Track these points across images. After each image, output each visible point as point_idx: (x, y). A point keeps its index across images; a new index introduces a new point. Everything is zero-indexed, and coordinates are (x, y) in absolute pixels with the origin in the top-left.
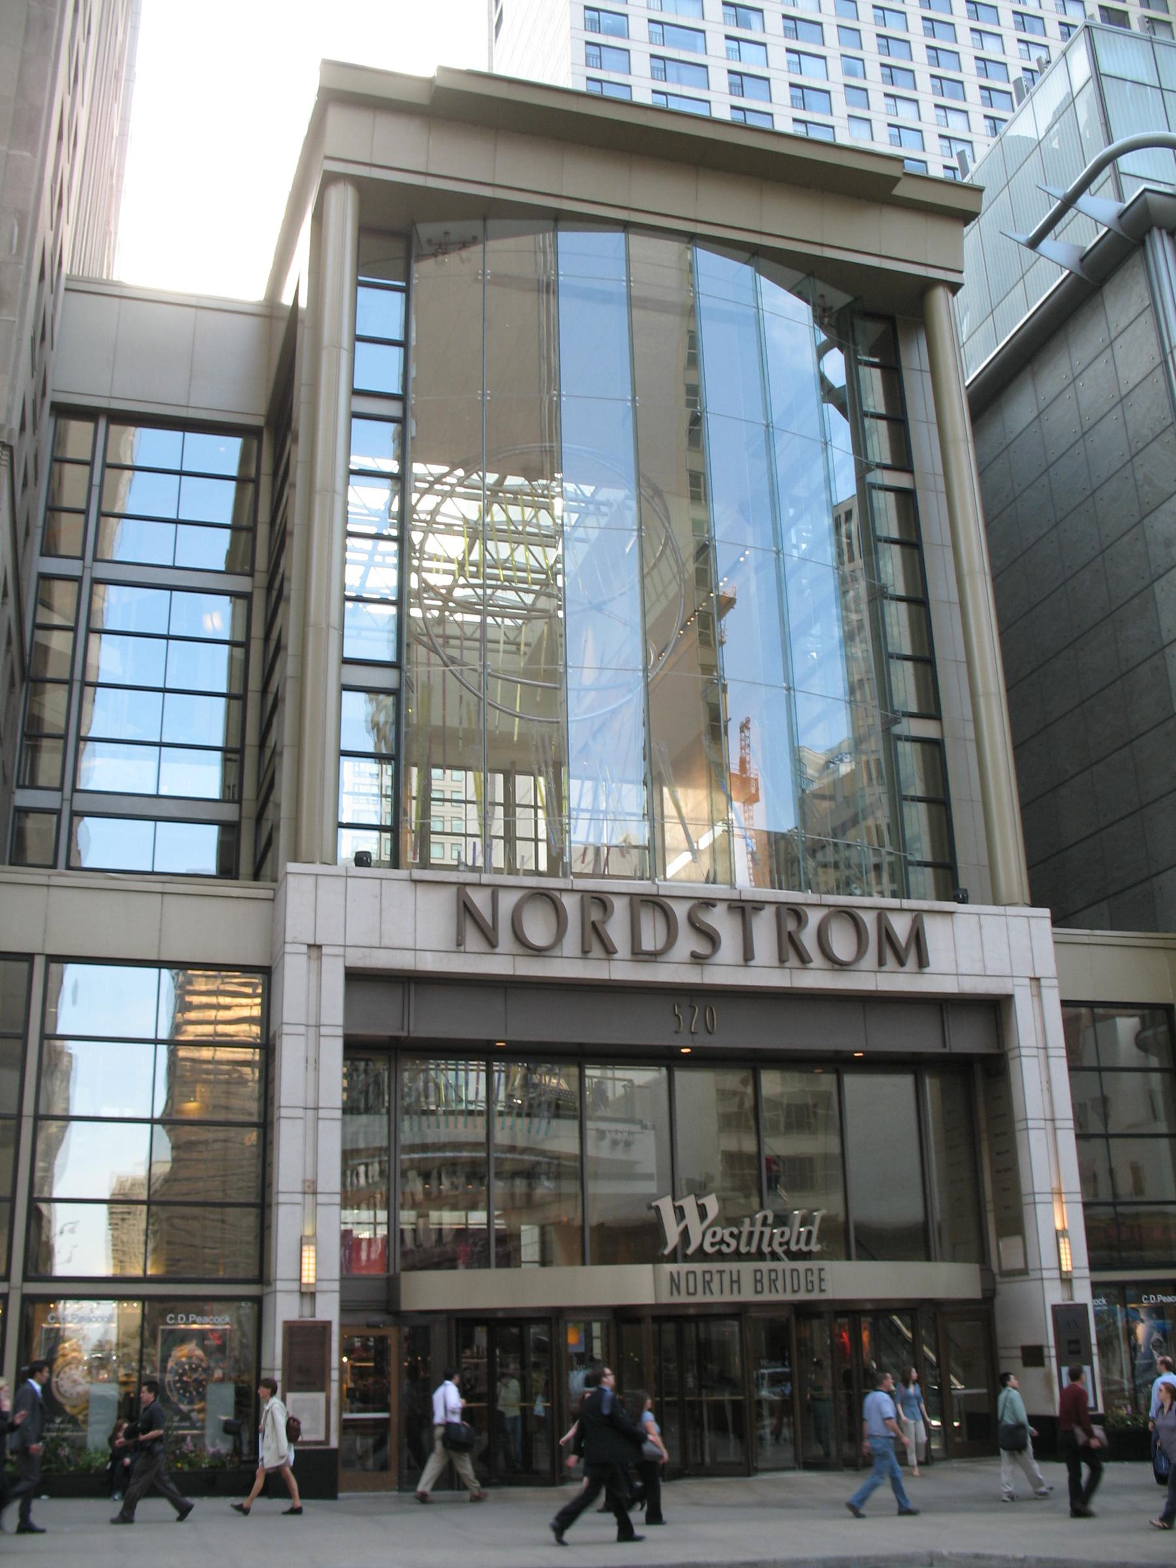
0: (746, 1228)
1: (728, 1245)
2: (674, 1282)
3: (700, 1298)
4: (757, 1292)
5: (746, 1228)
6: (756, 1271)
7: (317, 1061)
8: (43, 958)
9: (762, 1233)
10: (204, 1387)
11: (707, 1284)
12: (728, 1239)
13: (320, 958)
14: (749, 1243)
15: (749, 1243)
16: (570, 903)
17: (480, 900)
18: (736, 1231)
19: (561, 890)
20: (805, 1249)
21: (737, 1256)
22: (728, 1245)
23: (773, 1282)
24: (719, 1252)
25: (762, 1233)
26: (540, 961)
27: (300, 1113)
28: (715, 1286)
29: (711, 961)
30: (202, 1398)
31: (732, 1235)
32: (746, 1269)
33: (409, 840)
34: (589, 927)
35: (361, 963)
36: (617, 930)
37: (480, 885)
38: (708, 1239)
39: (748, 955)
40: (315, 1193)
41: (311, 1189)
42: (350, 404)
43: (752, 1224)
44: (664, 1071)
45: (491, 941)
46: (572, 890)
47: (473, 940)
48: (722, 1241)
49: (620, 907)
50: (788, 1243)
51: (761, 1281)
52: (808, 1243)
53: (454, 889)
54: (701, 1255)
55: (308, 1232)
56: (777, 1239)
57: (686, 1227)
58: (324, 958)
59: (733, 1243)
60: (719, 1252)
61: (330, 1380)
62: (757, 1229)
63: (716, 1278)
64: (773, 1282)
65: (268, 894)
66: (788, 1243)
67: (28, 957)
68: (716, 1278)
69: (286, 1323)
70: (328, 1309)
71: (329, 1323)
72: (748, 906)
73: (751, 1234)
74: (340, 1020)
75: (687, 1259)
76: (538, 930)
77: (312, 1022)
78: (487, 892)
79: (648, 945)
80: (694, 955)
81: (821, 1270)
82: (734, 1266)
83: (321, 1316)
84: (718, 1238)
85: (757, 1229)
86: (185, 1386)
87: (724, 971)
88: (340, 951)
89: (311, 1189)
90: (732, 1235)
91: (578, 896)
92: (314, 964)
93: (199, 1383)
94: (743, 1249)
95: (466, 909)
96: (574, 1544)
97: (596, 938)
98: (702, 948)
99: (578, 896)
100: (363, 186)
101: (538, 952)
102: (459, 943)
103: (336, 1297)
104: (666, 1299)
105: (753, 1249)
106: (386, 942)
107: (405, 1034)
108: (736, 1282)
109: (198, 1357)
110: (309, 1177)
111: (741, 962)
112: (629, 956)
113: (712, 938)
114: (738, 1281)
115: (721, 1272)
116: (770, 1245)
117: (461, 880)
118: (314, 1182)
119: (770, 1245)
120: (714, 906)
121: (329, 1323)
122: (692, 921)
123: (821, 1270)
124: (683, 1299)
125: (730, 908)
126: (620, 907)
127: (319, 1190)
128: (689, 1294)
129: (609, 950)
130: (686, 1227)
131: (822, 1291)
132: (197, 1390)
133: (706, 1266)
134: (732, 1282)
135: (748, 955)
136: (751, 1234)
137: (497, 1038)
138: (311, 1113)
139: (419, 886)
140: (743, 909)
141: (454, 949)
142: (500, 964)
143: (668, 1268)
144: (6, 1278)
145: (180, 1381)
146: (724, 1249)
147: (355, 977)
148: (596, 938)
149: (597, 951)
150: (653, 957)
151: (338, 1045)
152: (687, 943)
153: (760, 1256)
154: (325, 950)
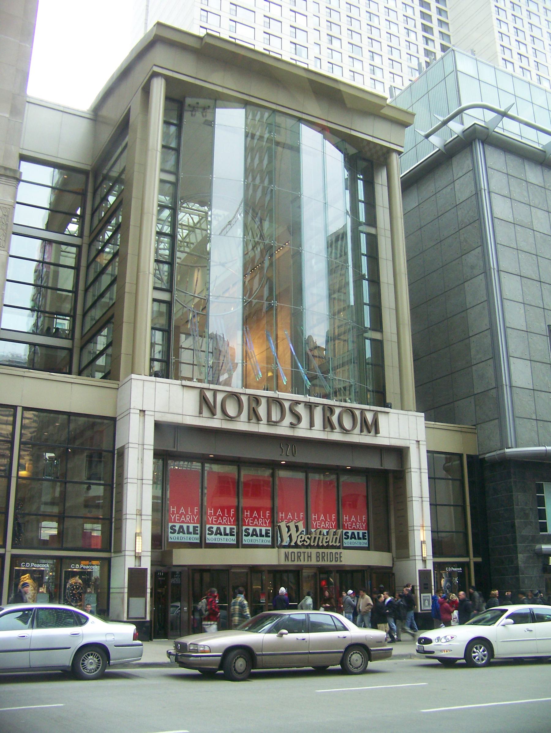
0: (313, 536)
1: (307, 542)
2: (286, 556)
3: (296, 563)
4: (317, 561)
5: (313, 536)
6: (317, 553)
7: (142, 459)
8: (21, 408)
9: (319, 538)
10: (81, 595)
11: (299, 557)
12: (306, 539)
13: (144, 415)
14: (314, 542)
15: (314, 542)
16: (244, 399)
17: (209, 395)
18: (310, 537)
19: (240, 393)
20: (335, 545)
21: (309, 546)
22: (307, 542)
23: (323, 557)
24: (303, 545)
25: (319, 538)
26: (274, 427)
27: (136, 481)
28: (302, 558)
29: (297, 426)
30: (81, 600)
31: (308, 538)
32: (314, 551)
33: (172, 368)
34: (327, 419)
35: (160, 419)
36: (262, 410)
37: (209, 389)
38: (299, 539)
39: (312, 424)
40: (141, 515)
41: (140, 513)
42: (159, 176)
43: (316, 534)
44: (365, 478)
45: (213, 413)
46: (245, 394)
47: (206, 412)
48: (304, 541)
49: (263, 401)
50: (328, 542)
51: (319, 557)
52: (335, 542)
53: (199, 390)
54: (296, 546)
55: (138, 531)
56: (325, 540)
57: (291, 534)
58: (146, 416)
59: (308, 541)
60: (303, 545)
61: (147, 593)
62: (318, 536)
63: (302, 555)
64: (323, 557)
65: (115, 386)
66: (328, 542)
67: (15, 407)
68: (302, 555)
69: (129, 569)
70: (146, 563)
71: (147, 569)
72: (313, 405)
73: (315, 538)
74: (152, 443)
75: (293, 547)
76: (231, 410)
77: (141, 443)
78: (212, 392)
79: (274, 419)
80: (291, 423)
81: (341, 553)
82: (309, 550)
83: (143, 566)
84: (303, 539)
85: (318, 536)
86: (74, 595)
87: (302, 431)
88: (152, 413)
89: (140, 513)
90: (308, 538)
91: (247, 397)
92: (142, 418)
93: (80, 594)
94: (312, 544)
95: (203, 400)
96: (404, 641)
97: (254, 415)
98: (295, 422)
99: (247, 397)
100: (168, 79)
101: (231, 419)
102: (201, 413)
103: (149, 558)
104: (283, 562)
105: (316, 545)
106: (171, 411)
107: (175, 450)
108: (310, 557)
109: (80, 583)
110: (139, 508)
111: (309, 428)
112: (266, 423)
113: (299, 418)
114: (311, 556)
115: (304, 553)
116: (322, 542)
117: (202, 387)
118: (141, 510)
119: (322, 542)
120: (300, 404)
121: (147, 569)
122: (291, 410)
123: (341, 553)
124: (290, 563)
125: (305, 405)
126: (263, 401)
127: (143, 514)
128: (292, 561)
129: (258, 419)
130: (291, 534)
131: (341, 561)
132: (79, 597)
133: (299, 550)
134: (308, 556)
135: (312, 424)
136: (315, 538)
137: (282, 460)
138: (139, 481)
139: (185, 387)
140: (311, 406)
141: (198, 415)
142: (216, 423)
143: (283, 551)
144: (4, 546)
145: (72, 593)
146: (305, 544)
147: (158, 425)
148: (254, 415)
149: (254, 420)
150: (276, 424)
151: (152, 453)
152: (288, 419)
153: (318, 547)
154: (146, 412)
